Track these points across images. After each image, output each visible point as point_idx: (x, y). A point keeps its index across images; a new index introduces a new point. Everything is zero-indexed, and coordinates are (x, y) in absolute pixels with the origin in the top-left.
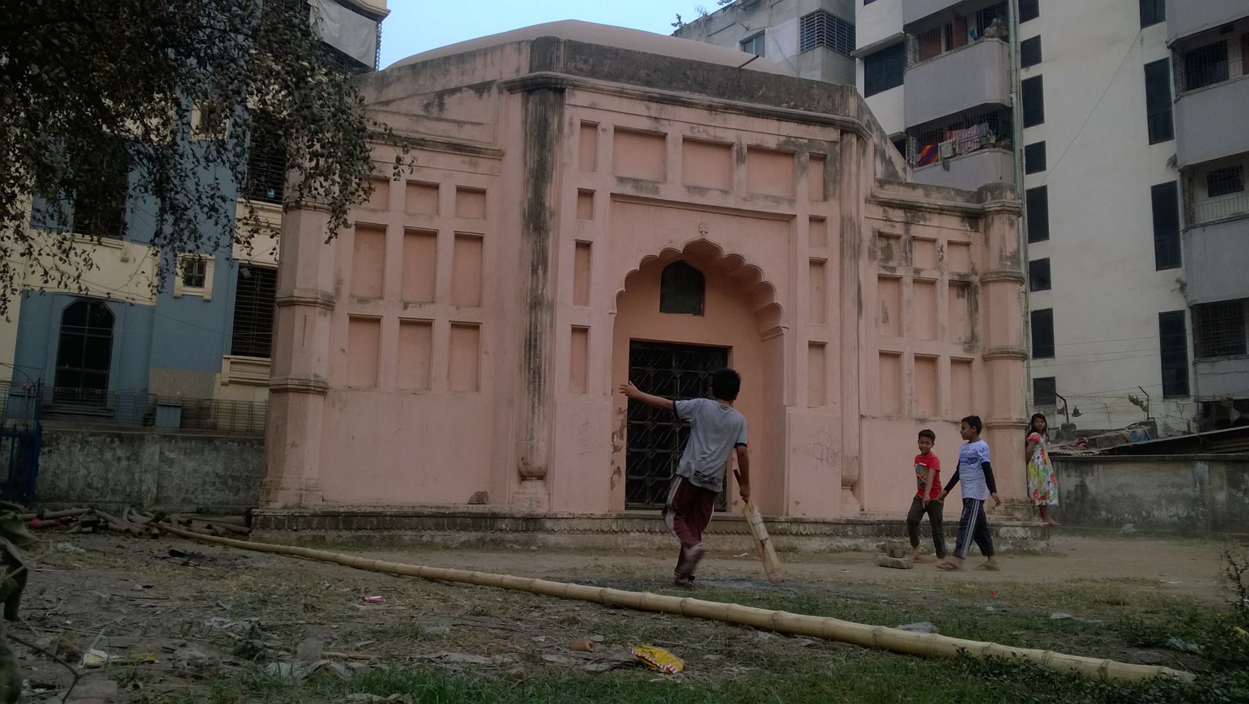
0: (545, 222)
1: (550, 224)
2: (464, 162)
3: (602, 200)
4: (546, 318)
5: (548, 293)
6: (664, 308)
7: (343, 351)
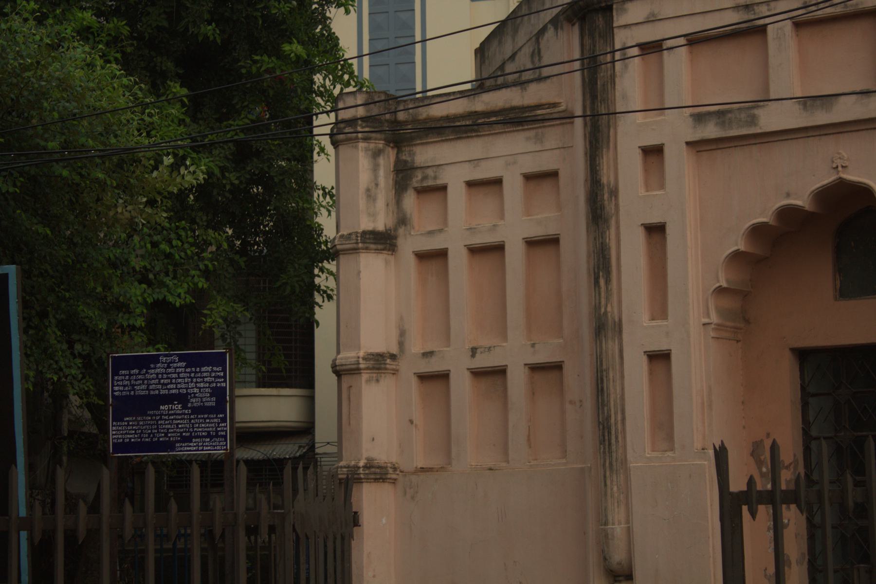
0: (602, 207)
1: (610, 208)
2: (528, 139)
3: (677, 159)
4: (611, 346)
5: (612, 310)
6: (845, 292)
7: (411, 422)
